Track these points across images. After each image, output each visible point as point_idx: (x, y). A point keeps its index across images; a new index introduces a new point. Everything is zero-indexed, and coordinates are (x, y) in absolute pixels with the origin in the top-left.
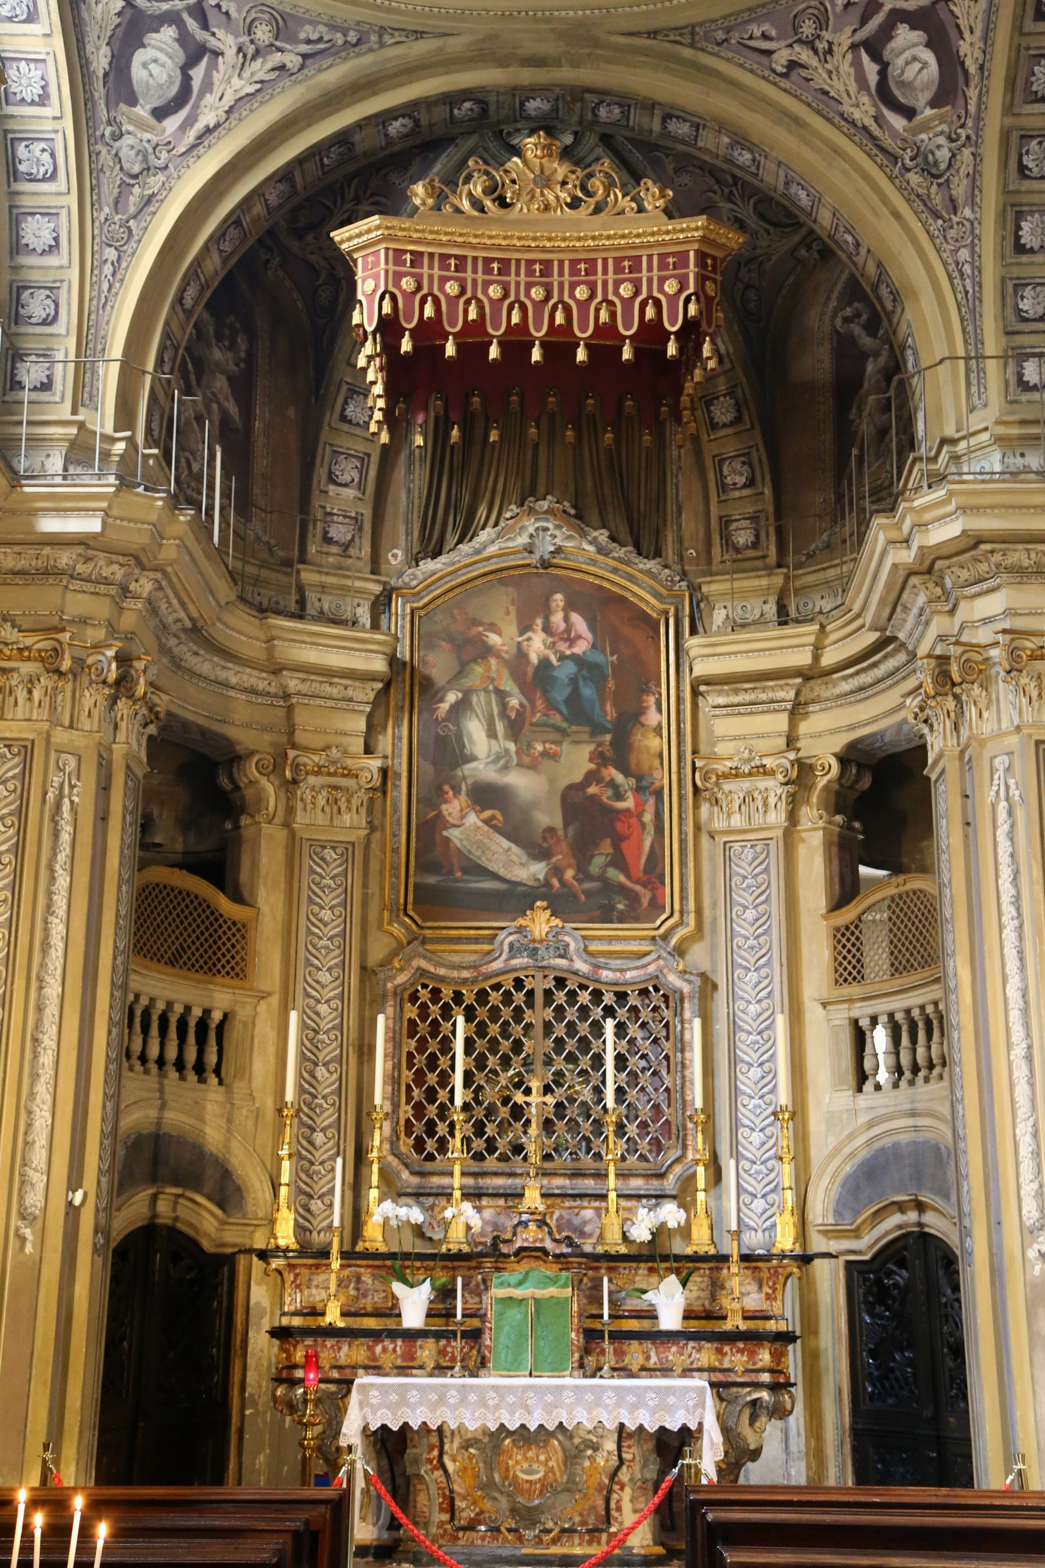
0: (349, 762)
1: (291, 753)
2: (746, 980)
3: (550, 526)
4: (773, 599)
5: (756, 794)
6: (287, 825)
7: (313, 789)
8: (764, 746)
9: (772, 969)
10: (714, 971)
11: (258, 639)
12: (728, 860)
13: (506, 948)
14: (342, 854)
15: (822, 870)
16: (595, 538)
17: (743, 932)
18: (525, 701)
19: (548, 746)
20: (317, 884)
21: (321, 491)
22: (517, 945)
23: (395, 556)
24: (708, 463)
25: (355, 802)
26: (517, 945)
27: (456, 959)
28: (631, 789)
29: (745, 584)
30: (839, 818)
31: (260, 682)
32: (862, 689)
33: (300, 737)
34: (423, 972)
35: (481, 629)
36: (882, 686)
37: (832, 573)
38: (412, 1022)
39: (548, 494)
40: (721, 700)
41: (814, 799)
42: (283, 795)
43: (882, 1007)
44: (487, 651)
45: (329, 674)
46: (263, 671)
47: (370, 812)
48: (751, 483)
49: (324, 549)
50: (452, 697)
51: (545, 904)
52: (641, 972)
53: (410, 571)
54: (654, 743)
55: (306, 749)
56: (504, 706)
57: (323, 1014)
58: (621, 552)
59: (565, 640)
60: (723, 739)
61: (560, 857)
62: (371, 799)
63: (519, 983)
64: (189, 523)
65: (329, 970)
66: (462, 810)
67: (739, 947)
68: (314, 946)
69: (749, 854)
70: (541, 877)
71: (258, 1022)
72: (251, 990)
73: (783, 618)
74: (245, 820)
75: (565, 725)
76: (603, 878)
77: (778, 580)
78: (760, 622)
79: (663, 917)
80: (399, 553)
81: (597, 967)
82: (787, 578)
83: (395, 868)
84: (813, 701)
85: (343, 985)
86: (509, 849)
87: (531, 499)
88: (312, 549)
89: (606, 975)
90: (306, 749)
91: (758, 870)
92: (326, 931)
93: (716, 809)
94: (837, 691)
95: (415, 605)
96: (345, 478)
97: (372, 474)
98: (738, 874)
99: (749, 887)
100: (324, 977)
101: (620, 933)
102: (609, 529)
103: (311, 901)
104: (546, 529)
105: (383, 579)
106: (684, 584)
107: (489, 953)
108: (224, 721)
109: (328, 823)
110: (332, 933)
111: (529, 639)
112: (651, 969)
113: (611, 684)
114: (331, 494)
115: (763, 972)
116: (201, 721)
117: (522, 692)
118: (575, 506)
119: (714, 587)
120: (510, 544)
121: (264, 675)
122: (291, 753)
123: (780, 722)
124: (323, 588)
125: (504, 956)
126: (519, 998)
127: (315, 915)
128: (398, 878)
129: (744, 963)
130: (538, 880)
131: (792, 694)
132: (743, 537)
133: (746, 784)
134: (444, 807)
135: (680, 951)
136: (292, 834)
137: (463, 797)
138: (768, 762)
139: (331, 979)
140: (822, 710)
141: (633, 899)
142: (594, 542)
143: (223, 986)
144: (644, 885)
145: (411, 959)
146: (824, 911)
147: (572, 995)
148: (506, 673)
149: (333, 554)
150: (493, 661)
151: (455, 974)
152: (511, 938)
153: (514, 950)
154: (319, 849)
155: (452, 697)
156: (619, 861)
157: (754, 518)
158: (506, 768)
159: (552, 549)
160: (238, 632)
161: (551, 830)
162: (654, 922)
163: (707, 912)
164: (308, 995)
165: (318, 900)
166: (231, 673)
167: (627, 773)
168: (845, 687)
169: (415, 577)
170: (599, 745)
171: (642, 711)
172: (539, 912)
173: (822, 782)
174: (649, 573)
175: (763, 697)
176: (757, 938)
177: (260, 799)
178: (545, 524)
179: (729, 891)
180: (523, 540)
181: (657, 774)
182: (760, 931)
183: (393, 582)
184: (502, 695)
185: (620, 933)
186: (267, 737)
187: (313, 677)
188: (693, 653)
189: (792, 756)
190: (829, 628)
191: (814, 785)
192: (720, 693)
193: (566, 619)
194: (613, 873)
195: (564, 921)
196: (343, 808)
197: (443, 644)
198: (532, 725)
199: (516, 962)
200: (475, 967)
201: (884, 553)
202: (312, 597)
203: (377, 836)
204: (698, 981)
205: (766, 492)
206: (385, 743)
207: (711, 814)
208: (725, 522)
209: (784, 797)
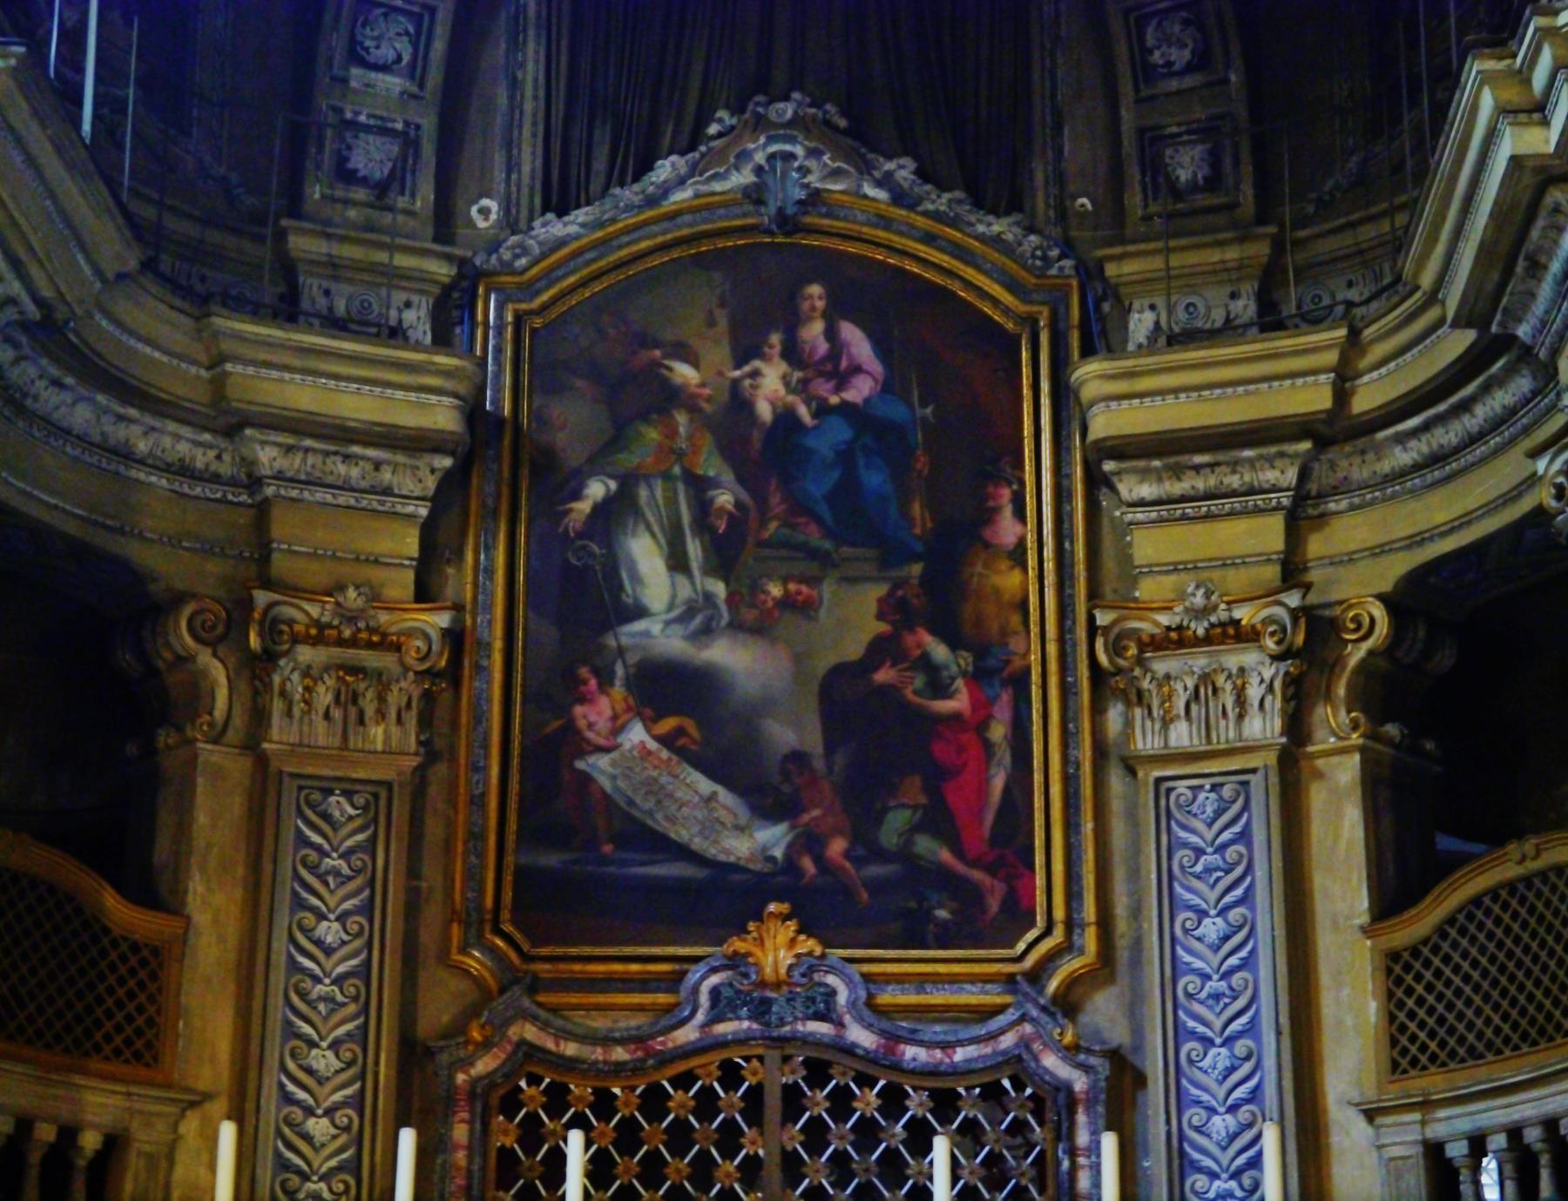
0: (384, 617)
1: (262, 597)
2: (1205, 1064)
3: (799, 150)
4: (1248, 288)
5: (1220, 680)
6: (252, 745)
7: (306, 673)
8: (1236, 580)
9: (1258, 1039)
10: (1139, 1046)
11: (193, 362)
12: (1164, 817)
13: (704, 999)
14: (365, 808)
15: (1360, 833)
16: (889, 175)
17: (1198, 964)
18: (745, 497)
19: (792, 587)
20: (313, 869)
21: (334, 79)
22: (727, 992)
23: (485, 212)
24: (1117, 26)
25: (394, 699)
26: (727, 992)
27: (599, 1023)
28: (964, 674)
29: (1193, 258)
30: (1392, 730)
31: (199, 452)
32: (1436, 459)
33: (280, 564)
34: (529, 1053)
35: (658, 353)
36: (1480, 450)
37: (1368, 232)
38: (506, 1154)
39: (792, 89)
40: (1147, 491)
41: (1341, 690)
42: (243, 687)
43: (1495, 1114)
44: (671, 396)
45: (340, 434)
46: (205, 429)
47: (425, 722)
48: (1200, 62)
49: (339, 193)
50: (597, 490)
51: (784, 908)
52: (987, 1049)
53: (514, 239)
54: (1010, 580)
55: (294, 590)
56: (703, 509)
57: (318, 1139)
58: (941, 202)
59: (828, 376)
60: (1152, 570)
61: (816, 813)
62: (427, 696)
63: (731, 1074)
64: (14, 72)
65: (335, 1046)
66: (615, 718)
67: (1189, 996)
68: (303, 995)
69: (1207, 802)
70: (778, 853)
71: (182, 1158)
72: (169, 1086)
73: (1270, 320)
74: (165, 738)
75: (827, 545)
76: (905, 855)
77: (1260, 250)
78: (1229, 330)
79: (1031, 936)
80: (492, 204)
81: (893, 1039)
82: (1278, 246)
83: (476, 836)
84: (1335, 491)
85: (362, 1076)
86: (713, 797)
87: (760, 98)
88: (315, 192)
89: (910, 1052)
90: (294, 590)
91: (1226, 836)
92: (328, 964)
93: (1138, 712)
94: (1385, 466)
95: (524, 306)
96: (385, 53)
97: (439, 46)
98: (1185, 845)
99: (1208, 870)
100: (324, 1060)
101: (941, 968)
102: (916, 158)
103: (299, 904)
104: (789, 157)
105: (458, 252)
106: (1068, 263)
107: (670, 1009)
108: (121, 531)
109: (337, 741)
110: (341, 969)
111: (756, 374)
112: (1007, 1041)
113: (922, 463)
114: (353, 84)
115: (1241, 1047)
116: (71, 528)
117: (741, 479)
118: (843, 114)
119: (1130, 268)
120: (718, 187)
121: (207, 437)
122: (262, 597)
123: (1269, 533)
124: (334, 268)
125: (700, 1017)
126: (731, 1101)
127: (306, 931)
128: (482, 856)
129: (1201, 1029)
130: (772, 859)
131: (1291, 476)
132: (1187, 165)
133: (1200, 661)
134: (579, 710)
135: (1067, 1005)
136: (262, 761)
137: (618, 690)
138: (1244, 614)
139: (338, 1065)
140: (1353, 508)
141: (966, 896)
142: (885, 182)
143: (104, 1077)
144: (990, 869)
145: (507, 1023)
146: (1364, 919)
147: (841, 1102)
148: (707, 442)
149: (355, 204)
150: (681, 418)
151: (598, 1054)
152: (715, 979)
153: (722, 1005)
154: (316, 796)
155: (597, 490)
156: (937, 821)
157: (1206, 132)
158: (706, 632)
159: (800, 194)
160: (148, 341)
161: (797, 758)
162: (1011, 945)
163: (1122, 925)
164: (288, 1099)
165: (315, 901)
166: (136, 430)
167: (954, 644)
168: (1403, 457)
169: (525, 251)
170: (896, 585)
171: (989, 516)
172: (772, 925)
173: (1356, 655)
174: (996, 241)
175: (1234, 481)
176: (1226, 976)
177: (197, 695)
178: (788, 147)
179: (1167, 880)
180: (743, 178)
181: (1016, 644)
182: (1233, 961)
183: (478, 262)
184: (699, 486)
185: (941, 968)
186: (214, 567)
187: (308, 442)
188: (1088, 392)
189: (1293, 599)
190: (1368, 333)
191: (1340, 661)
192: (1145, 474)
193: (831, 333)
194: (924, 845)
195: (827, 944)
196: (370, 710)
197: (579, 383)
198: (761, 544)
199: (724, 1028)
200: (636, 1039)
201: (1491, 136)
202: (312, 287)
203: (441, 769)
204: (1103, 1067)
205: (1233, 78)
206: (459, 581)
207: (1128, 723)
208: (1153, 143)
209: (1278, 685)
